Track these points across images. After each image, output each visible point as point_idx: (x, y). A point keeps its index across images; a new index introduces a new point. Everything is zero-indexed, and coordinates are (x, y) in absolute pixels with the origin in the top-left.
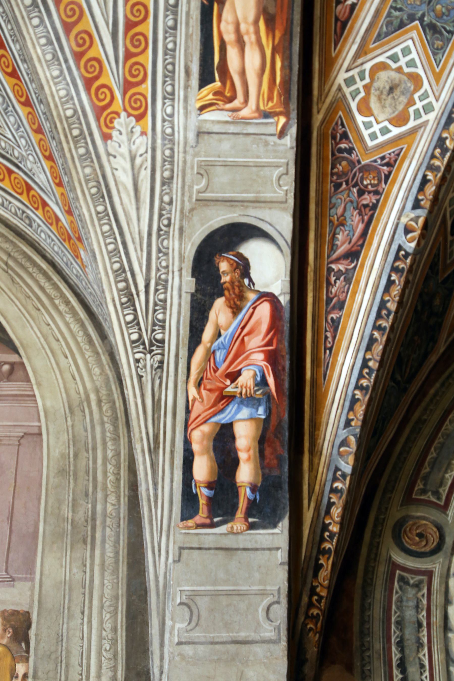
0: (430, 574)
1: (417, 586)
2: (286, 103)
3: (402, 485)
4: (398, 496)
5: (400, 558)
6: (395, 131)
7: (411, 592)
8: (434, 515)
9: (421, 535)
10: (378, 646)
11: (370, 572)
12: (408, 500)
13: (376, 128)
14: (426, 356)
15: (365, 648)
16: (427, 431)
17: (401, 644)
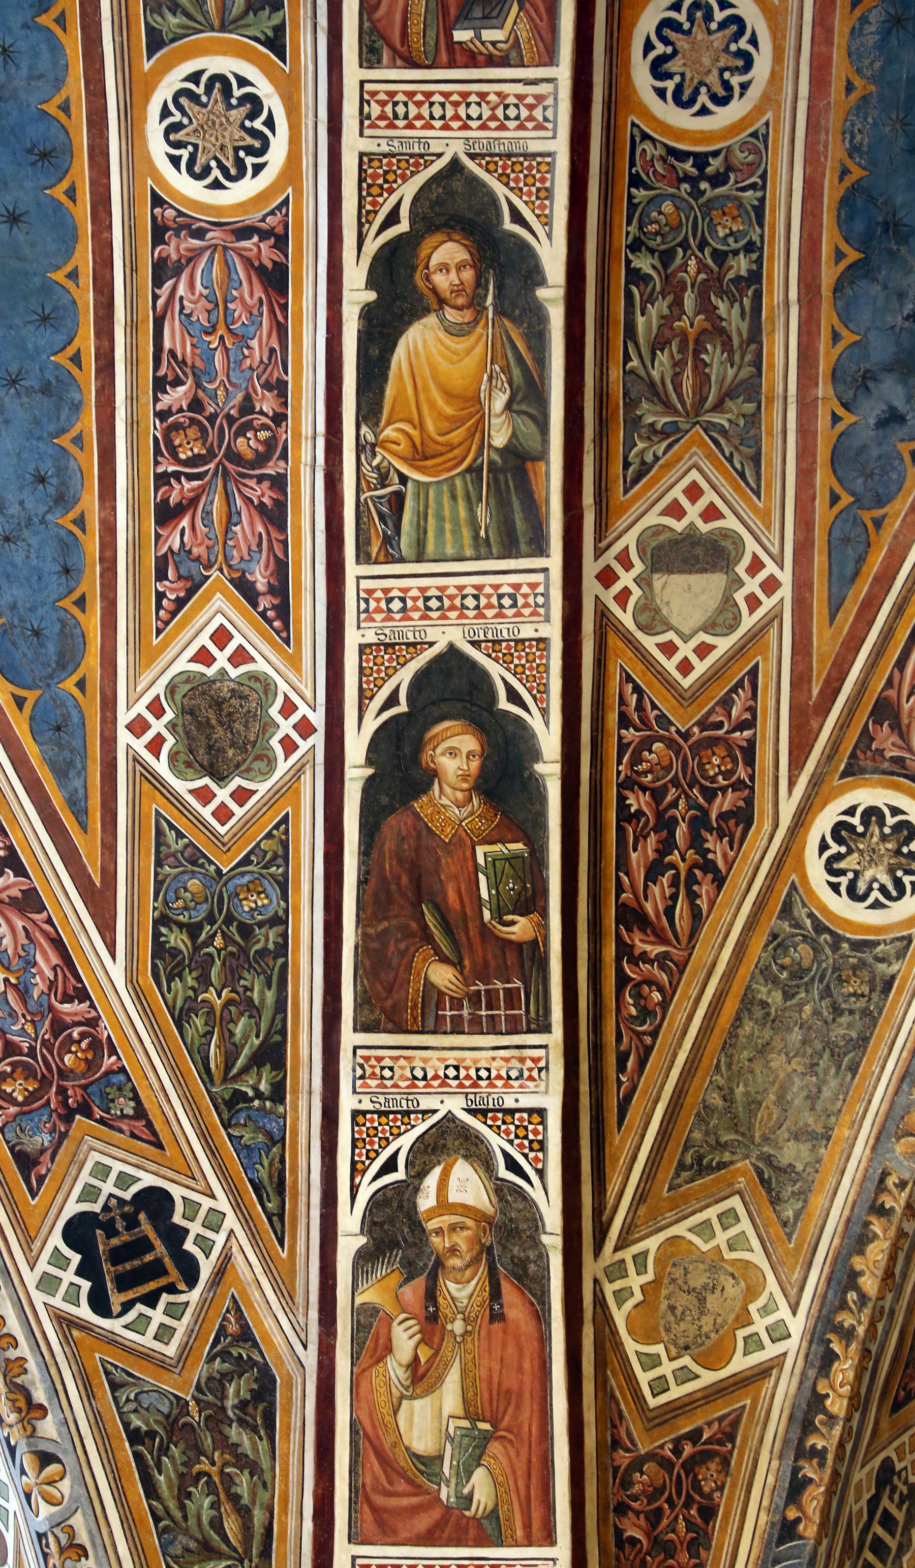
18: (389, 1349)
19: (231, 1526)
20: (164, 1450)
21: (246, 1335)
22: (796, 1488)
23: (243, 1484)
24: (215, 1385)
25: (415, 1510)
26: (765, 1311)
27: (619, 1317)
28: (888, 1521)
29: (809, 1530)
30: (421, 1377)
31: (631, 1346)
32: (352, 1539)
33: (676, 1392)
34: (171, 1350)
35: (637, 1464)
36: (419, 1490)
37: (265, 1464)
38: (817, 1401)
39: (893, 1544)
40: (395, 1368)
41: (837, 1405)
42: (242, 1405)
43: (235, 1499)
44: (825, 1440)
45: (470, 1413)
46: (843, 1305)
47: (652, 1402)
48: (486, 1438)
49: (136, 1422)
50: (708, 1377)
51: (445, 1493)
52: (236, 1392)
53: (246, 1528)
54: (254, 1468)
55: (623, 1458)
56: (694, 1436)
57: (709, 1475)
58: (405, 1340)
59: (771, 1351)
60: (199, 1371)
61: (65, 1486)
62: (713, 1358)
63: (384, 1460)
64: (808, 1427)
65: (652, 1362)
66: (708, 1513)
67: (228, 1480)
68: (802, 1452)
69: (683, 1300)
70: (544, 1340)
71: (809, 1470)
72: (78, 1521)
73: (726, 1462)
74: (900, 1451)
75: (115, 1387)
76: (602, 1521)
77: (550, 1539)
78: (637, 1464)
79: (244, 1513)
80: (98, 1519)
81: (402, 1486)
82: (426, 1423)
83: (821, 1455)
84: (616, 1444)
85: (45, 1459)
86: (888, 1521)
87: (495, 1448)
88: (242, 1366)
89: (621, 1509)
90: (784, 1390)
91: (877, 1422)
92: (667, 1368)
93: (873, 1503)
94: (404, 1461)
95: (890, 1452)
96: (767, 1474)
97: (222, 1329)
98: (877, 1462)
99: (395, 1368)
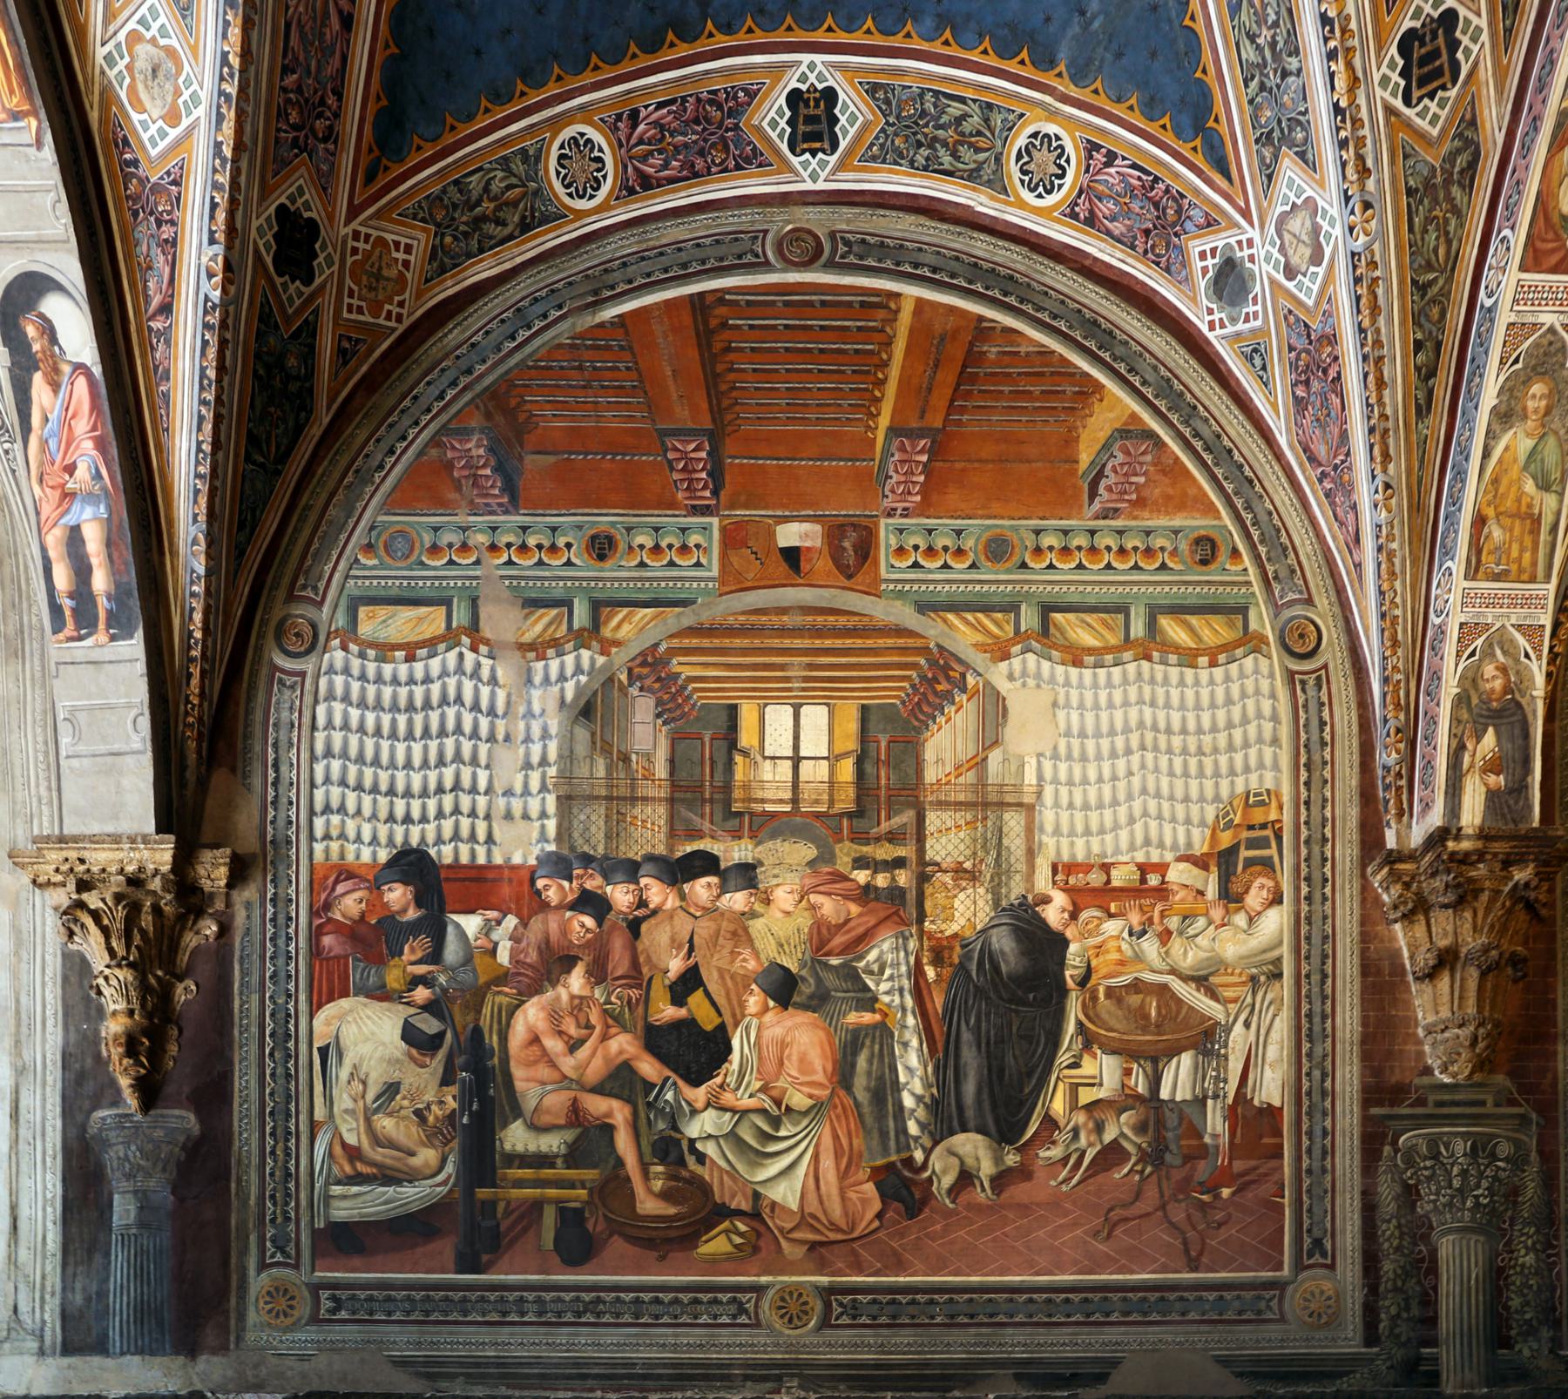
0: (303, 674)
1: (292, 687)
2: (30, 98)
3: (286, 581)
4: (281, 594)
5: (281, 661)
6: (173, 133)
7: (287, 693)
8: (310, 611)
9: (297, 635)
10: (258, 748)
11: (254, 674)
12: (291, 598)
13: (153, 129)
14: (299, 429)
15: (247, 750)
16: (312, 518)
17: (276, 745)
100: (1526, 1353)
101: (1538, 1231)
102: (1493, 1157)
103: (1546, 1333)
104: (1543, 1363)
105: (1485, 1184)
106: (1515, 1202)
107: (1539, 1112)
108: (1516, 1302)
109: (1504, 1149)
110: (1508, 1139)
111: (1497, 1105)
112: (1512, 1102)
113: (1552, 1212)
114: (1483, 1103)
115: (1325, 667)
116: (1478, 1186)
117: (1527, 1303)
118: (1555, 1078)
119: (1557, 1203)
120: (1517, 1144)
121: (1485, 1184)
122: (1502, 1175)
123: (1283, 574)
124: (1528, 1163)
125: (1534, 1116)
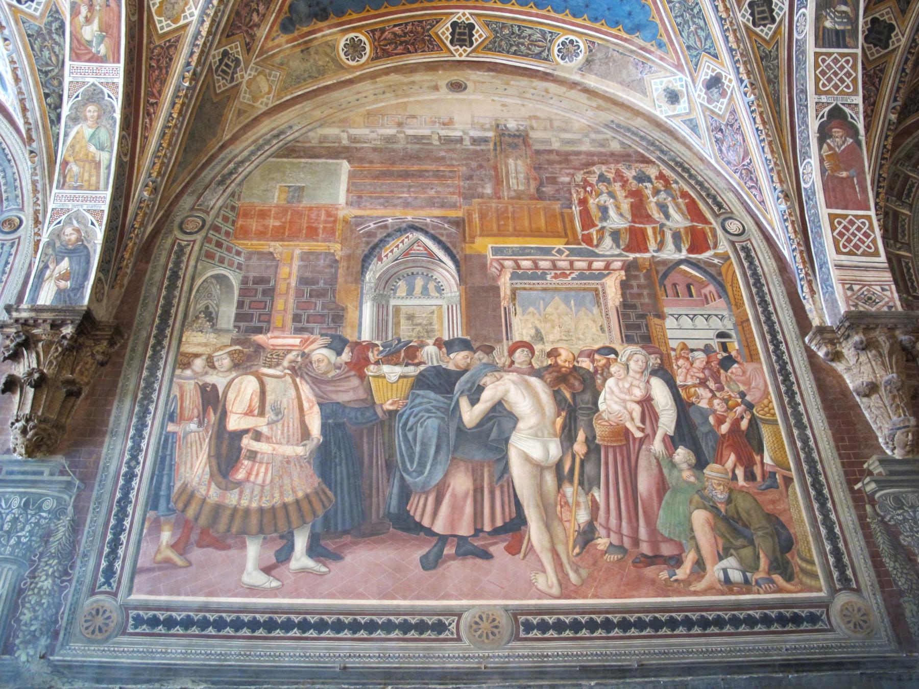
18: (79, 13)
19: (54, 59)
20: (36, 39)
21: (57, 11)
22: (192, 53)
23: (57, 49)
24: (50, 23)
25: (86, 54)
26: (189, 9)
27: (153, 10)
28: (227, 65)
29: (193, 64)
30: (88, 20)
31: (156, 18)
32: (70, 60)
33: (166, 30)
34: (38, 14)
35: (155, 48)
36: (87, 49)
37: (62, 44)
38: (199, 32)
39: (230, 72)
40: (81, 18)
41: (204, 33)
42: (57, 29)
43: (55, 52)
44: (200, 42)
45: (101, 30)
46: (208, 8)
47: (160, 32)
48: (104, 36)
49: (29, 32)
50: (174, 26)
51: (94, 50)
52: (55, 25)
53: (58, 60)
54: (59, 45)
55: (152, 46)
56: (169, 41)
57: (172, 51)
58: (84, 10)
59: (190, 19)
60: (45, 20)
61: (11, 47)
62: (175, 21)
63: (78, 40)
64: (196, 39)
65: (160, 22)
66: (171, 60)
67: (53, 48)
68: (195, 45)
69: (169, 6)
70: (120, 12)
71: (195, 49)
72: (14, 55)
73: (176, 47)
74: (231, 48)
75: (23, 23)
76: (146, 61)
77: (119, 62)
78: (155, 48)
79: (57, 56)
80: (19, 55)
81: (82, 48)
82: (89, 32)
83: (198, 45)
84: (151, 42)
85: (6, 40)
86: (227, 65)
87: (106, 39)
88: (56, 19)
89: (151, 59)
90: (191, 30)
91: (220, 39)
92: (164, 24)
93: (221, 61)
94: (83, 42)
95: (227, 48)
96: (185, 50)
97: (51, 10)
98: (222, 50)
99: (81, 18)
100: (23, 658)
101: (59, 563)
102: (40, 508)
103: (44, 642)
104: (34, 668)
105: (28, 528)
106: (47, 542)
107: (82, 480)
108: (27, 616)
109: (49, 504)
110: (53, 497)
111: (52, 474)
112: (63, 473)
113: (74, 548)
114: (41, 473)
115: (19, 238)
116: (22, 529)
117: (36, 618)
118: (99, 458)
119: (79, 542)
120: (59, 500)
121: (28, 528)
122: (43, 522)
123: (12, 196)
124: (65, 513)
125: (77, 482)
